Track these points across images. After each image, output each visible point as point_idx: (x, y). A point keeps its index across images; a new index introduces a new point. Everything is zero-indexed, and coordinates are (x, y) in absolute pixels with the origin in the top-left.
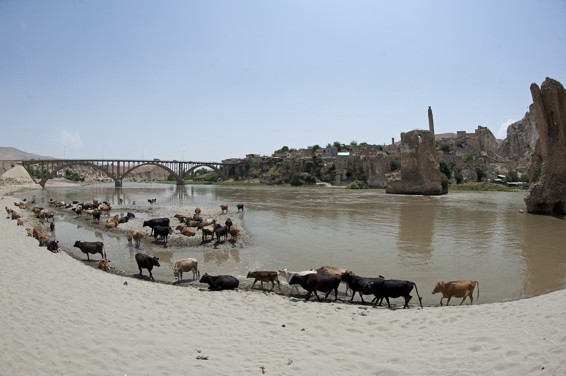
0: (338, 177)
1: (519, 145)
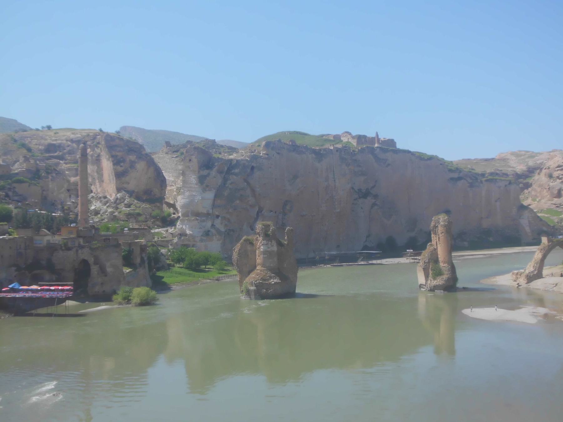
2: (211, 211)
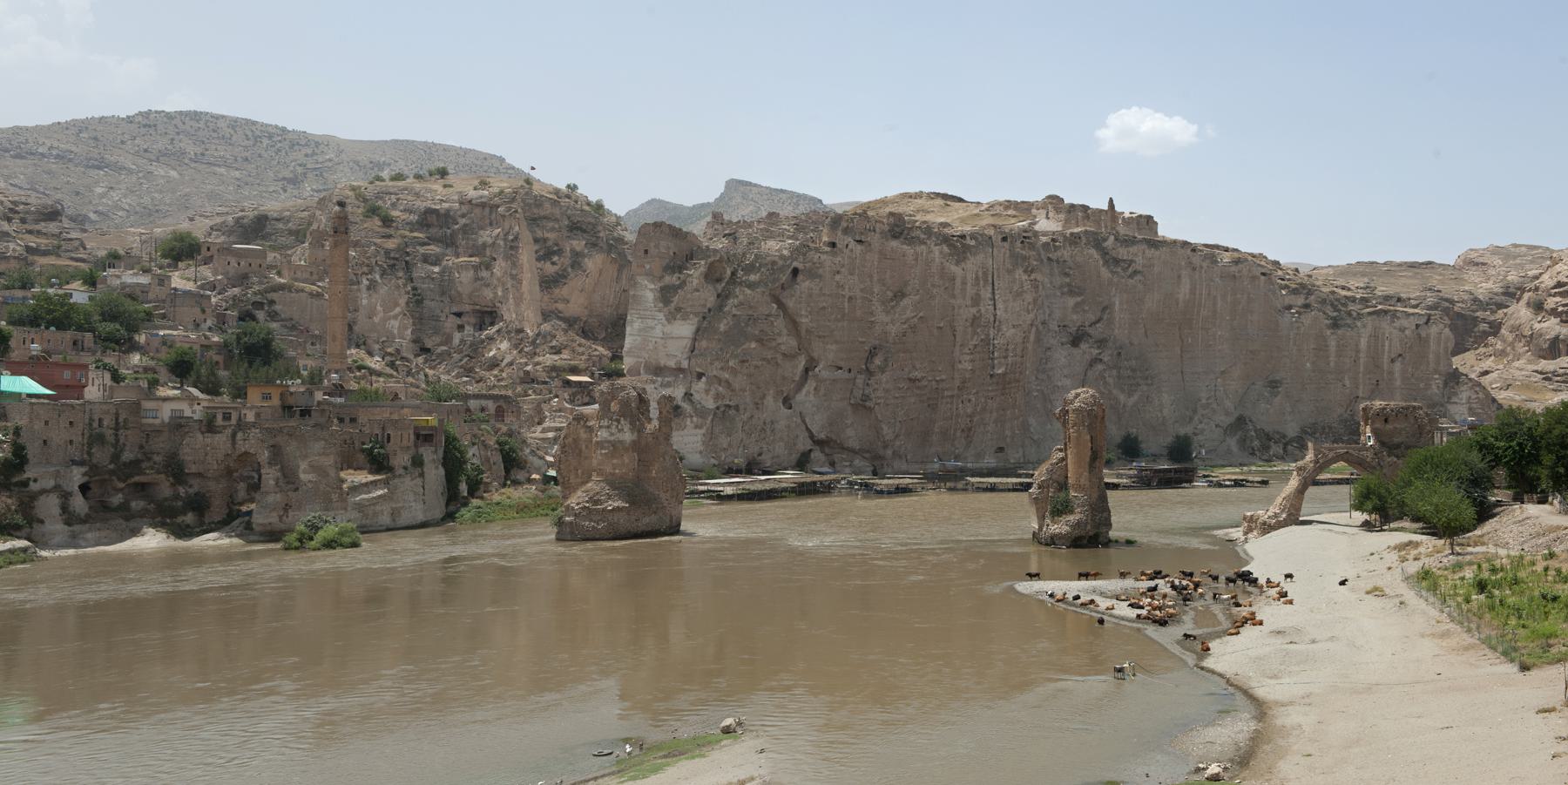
0: (49, 506)
2: (685, 364)
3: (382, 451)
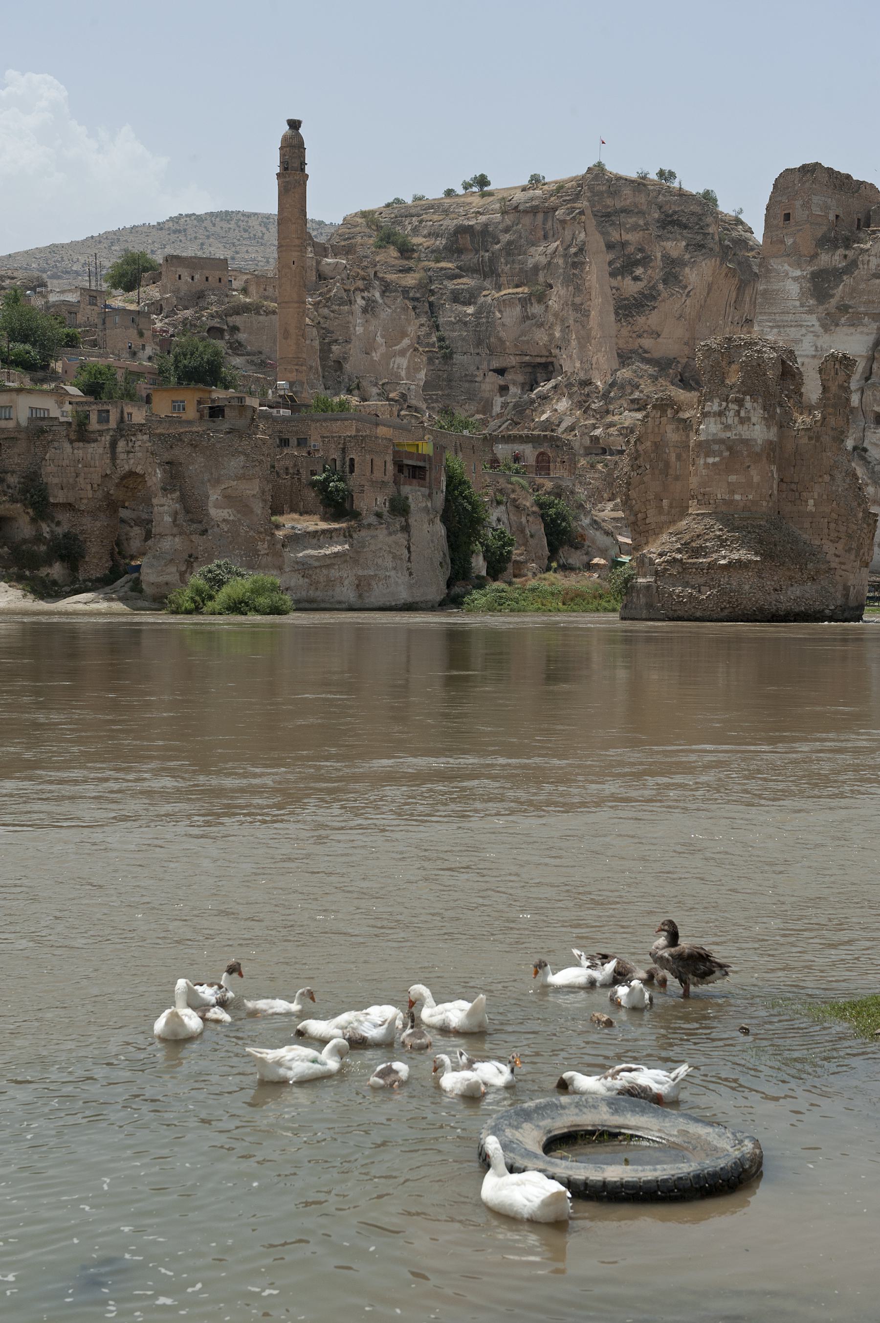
1: (448, 358)
3: (341, 485)
